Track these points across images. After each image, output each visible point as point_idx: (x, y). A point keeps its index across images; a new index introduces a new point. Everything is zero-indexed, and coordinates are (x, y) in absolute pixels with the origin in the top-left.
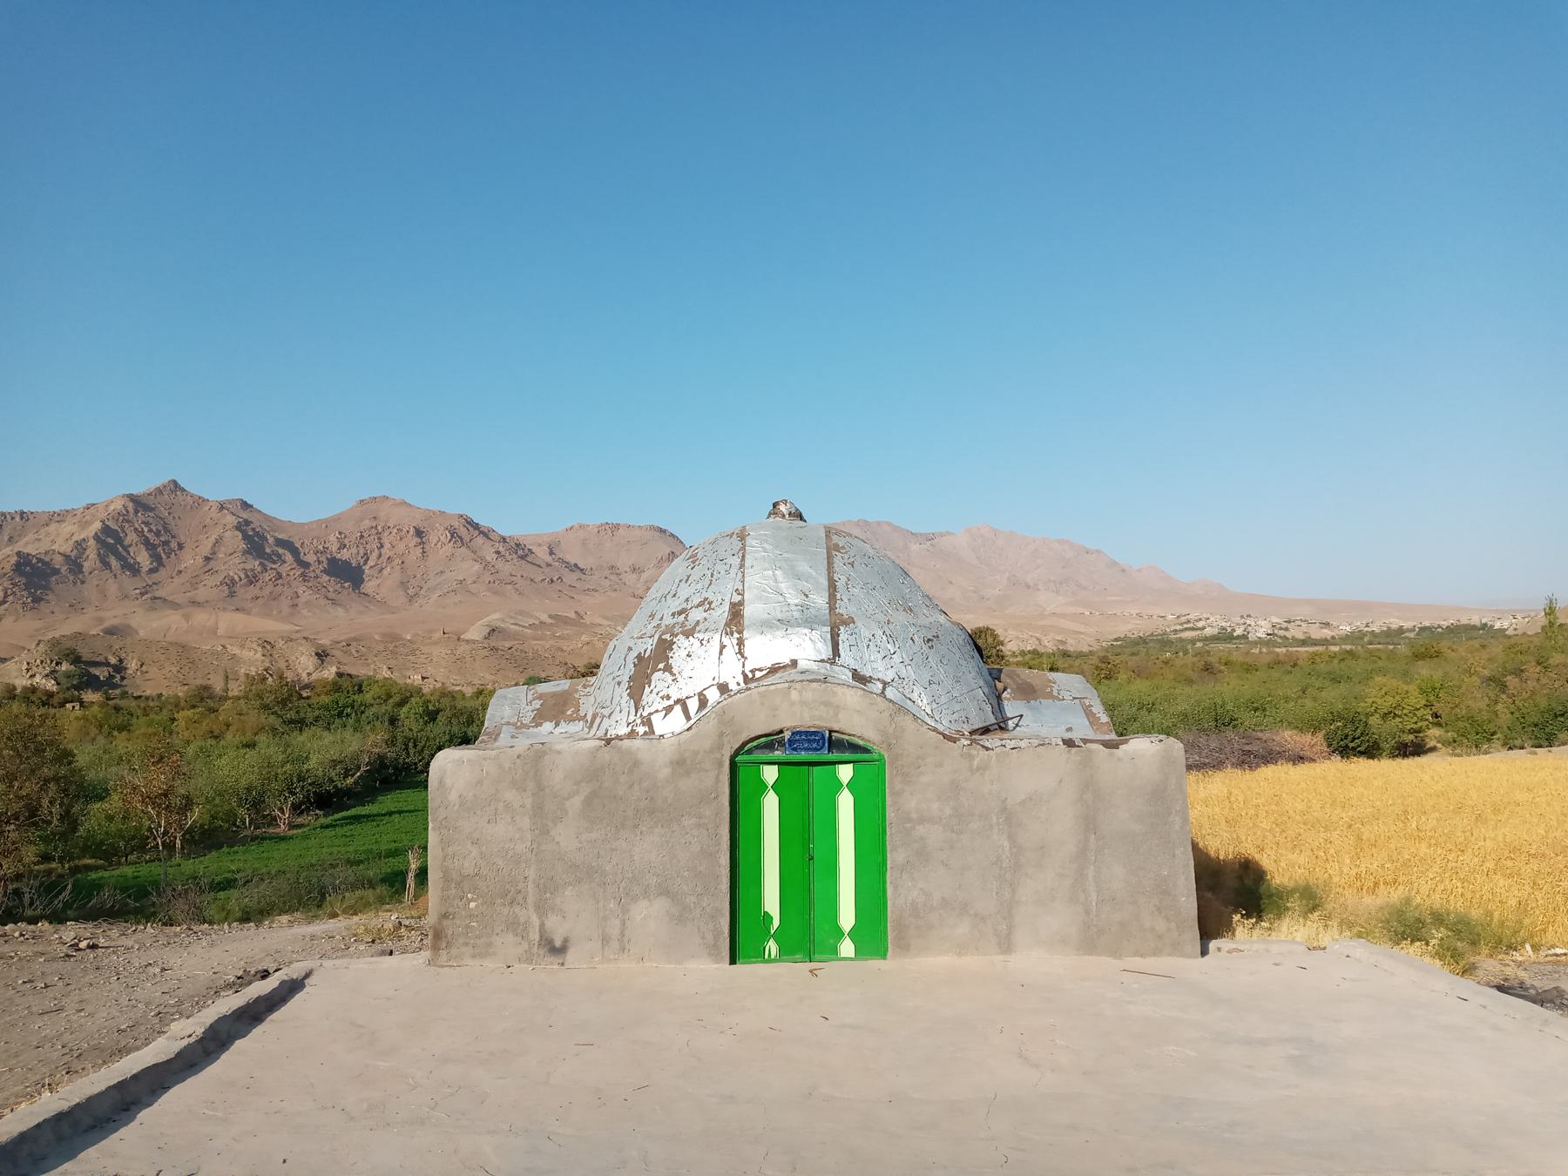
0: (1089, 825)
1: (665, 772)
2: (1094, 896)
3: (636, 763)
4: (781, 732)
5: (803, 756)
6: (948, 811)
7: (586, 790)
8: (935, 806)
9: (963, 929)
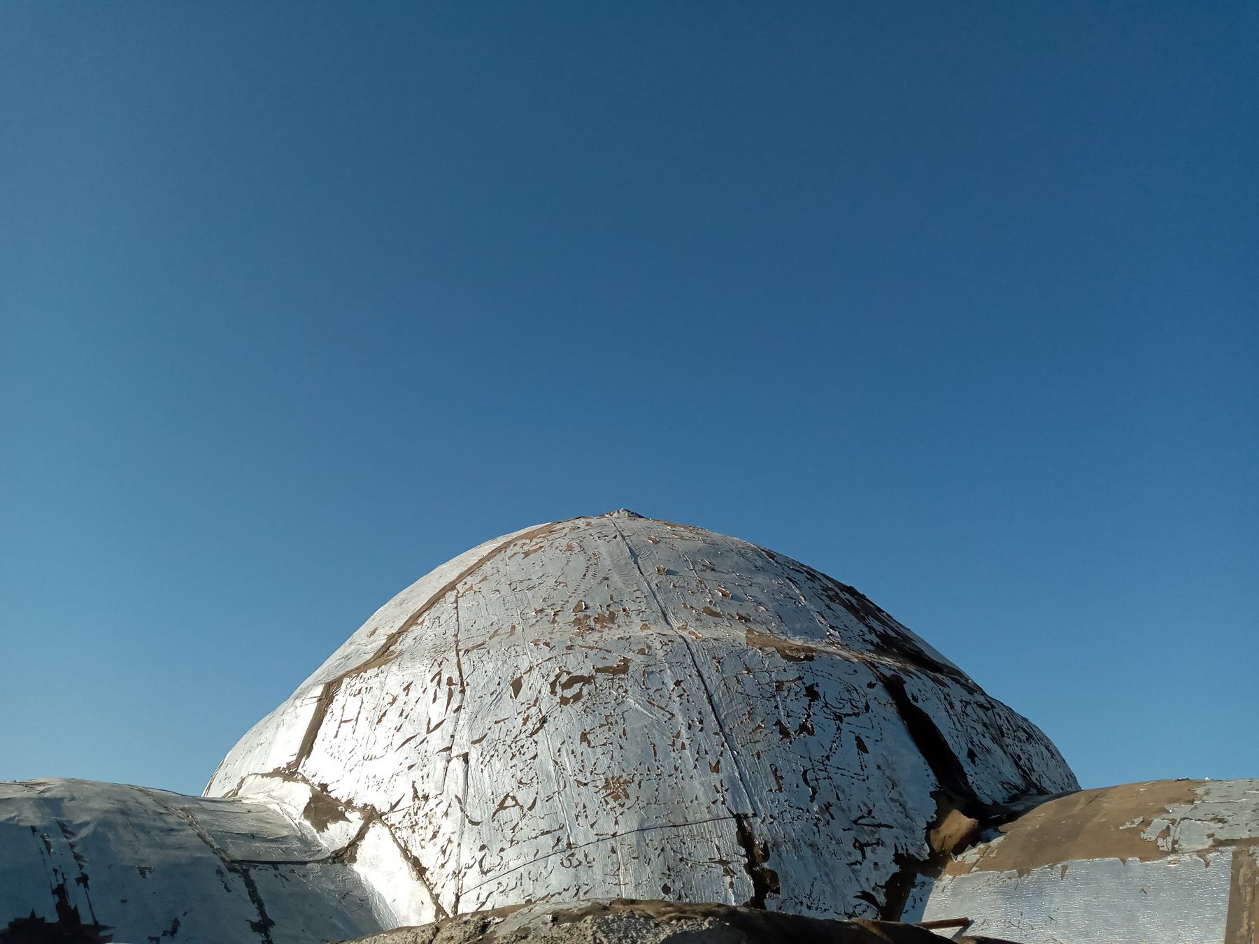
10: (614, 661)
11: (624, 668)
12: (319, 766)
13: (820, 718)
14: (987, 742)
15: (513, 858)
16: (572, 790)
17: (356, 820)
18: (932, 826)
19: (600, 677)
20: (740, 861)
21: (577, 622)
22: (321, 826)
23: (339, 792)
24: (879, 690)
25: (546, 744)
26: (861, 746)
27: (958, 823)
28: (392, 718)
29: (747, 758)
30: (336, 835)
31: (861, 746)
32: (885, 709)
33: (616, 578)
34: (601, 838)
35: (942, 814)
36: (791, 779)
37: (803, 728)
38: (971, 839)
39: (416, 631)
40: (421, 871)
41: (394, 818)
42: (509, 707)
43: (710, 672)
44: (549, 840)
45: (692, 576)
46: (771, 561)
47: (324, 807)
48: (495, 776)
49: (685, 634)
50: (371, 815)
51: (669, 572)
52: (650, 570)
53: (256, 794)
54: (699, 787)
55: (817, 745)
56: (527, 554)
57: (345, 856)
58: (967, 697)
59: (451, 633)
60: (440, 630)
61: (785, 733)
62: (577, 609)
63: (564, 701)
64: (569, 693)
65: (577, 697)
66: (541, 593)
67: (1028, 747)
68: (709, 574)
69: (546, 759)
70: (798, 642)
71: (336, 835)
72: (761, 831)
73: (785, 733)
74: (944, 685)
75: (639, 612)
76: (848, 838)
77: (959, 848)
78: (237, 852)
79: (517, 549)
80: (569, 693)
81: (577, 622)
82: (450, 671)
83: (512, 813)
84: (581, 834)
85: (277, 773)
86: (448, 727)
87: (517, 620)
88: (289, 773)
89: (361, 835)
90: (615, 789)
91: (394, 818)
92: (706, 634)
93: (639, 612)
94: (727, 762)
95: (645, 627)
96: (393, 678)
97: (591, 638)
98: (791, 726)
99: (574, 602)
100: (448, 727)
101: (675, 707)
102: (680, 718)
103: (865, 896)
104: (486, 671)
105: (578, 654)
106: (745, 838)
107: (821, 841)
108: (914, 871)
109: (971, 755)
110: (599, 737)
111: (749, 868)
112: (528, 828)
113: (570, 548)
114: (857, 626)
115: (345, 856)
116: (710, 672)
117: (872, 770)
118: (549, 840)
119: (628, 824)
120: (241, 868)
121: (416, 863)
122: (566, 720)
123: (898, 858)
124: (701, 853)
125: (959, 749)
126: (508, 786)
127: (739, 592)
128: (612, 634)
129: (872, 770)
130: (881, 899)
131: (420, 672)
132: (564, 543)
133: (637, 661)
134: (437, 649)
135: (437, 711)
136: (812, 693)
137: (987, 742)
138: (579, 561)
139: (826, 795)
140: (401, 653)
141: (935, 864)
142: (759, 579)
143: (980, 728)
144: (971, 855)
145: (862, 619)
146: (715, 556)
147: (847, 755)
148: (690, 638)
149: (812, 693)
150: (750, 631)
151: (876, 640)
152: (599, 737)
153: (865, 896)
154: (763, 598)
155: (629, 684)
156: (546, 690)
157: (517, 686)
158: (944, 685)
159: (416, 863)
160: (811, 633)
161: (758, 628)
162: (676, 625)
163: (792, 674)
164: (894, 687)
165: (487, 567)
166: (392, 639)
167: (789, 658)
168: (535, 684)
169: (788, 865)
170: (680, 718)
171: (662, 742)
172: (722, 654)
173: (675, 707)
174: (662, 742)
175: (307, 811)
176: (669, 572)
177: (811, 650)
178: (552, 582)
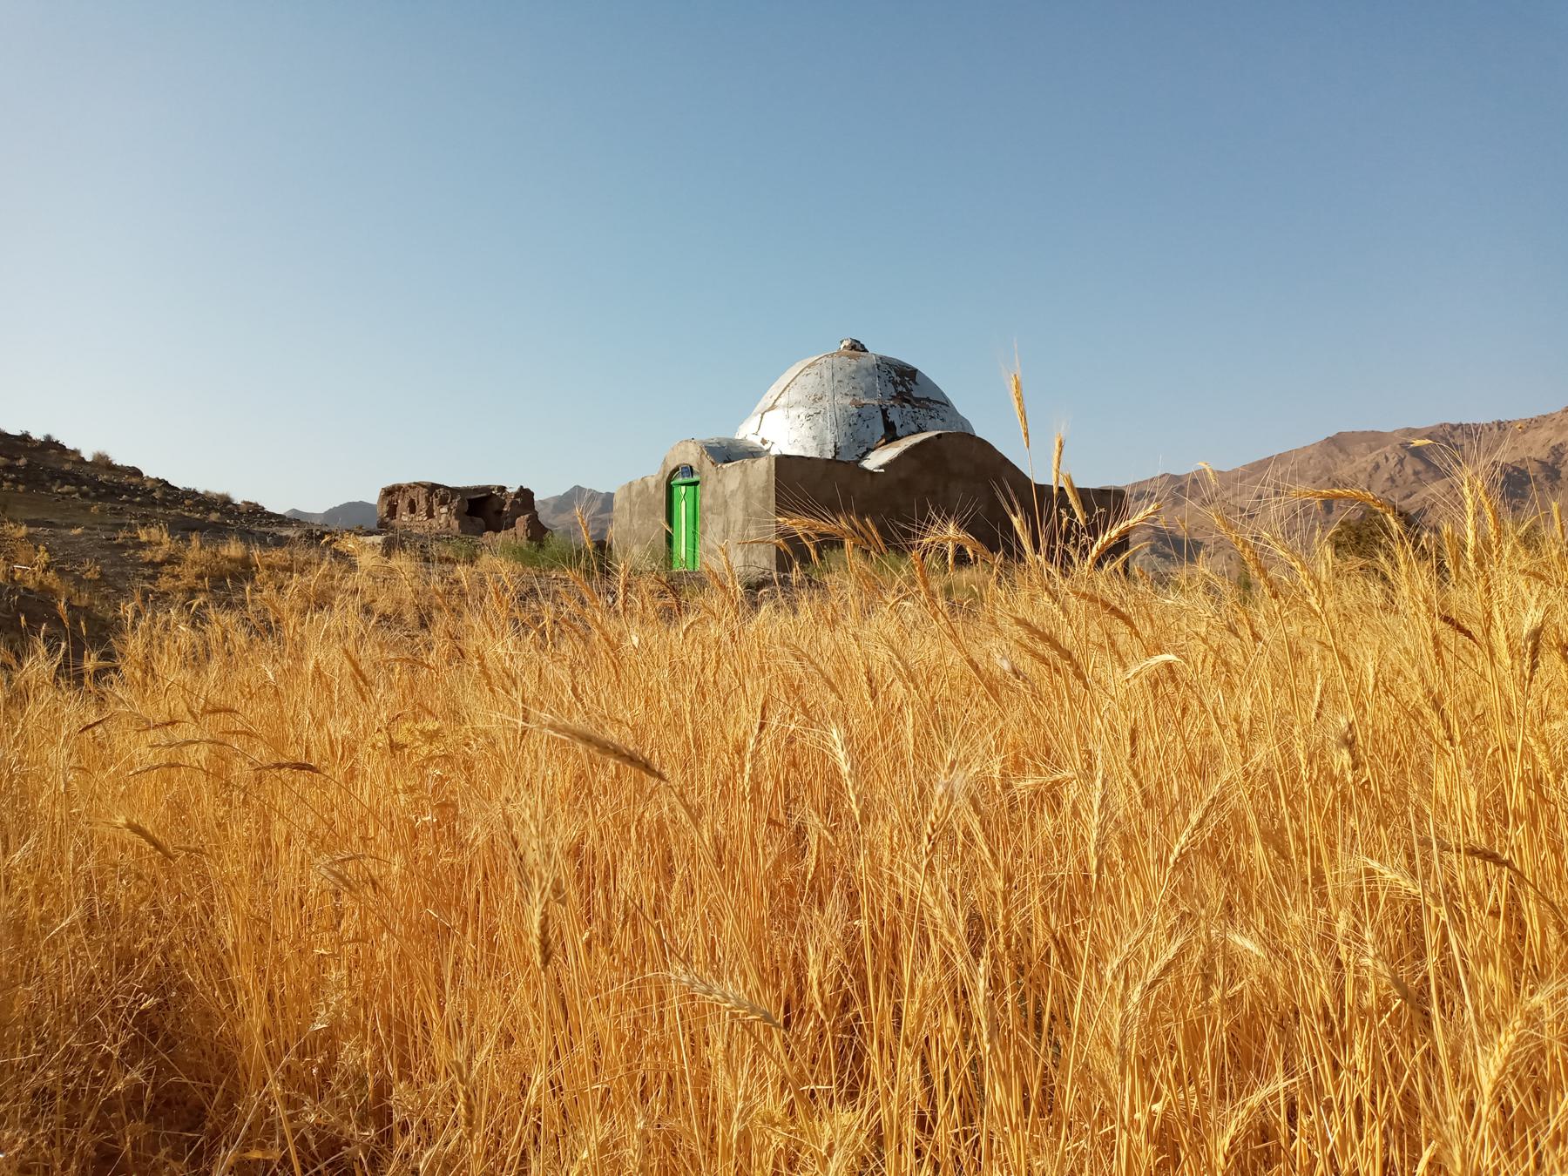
0: (746, 509)
4: (676, 469)
5: (687, 480)
32: (879, 416)
47: (764, 442)
54: (829, 437)
71: (766, 447)
104: (793, 413)
108: (869, 450)
114: (891, 390)
122: (808, 424)
125: (897, 425)
164: (884, 412)
169: (843, 451)
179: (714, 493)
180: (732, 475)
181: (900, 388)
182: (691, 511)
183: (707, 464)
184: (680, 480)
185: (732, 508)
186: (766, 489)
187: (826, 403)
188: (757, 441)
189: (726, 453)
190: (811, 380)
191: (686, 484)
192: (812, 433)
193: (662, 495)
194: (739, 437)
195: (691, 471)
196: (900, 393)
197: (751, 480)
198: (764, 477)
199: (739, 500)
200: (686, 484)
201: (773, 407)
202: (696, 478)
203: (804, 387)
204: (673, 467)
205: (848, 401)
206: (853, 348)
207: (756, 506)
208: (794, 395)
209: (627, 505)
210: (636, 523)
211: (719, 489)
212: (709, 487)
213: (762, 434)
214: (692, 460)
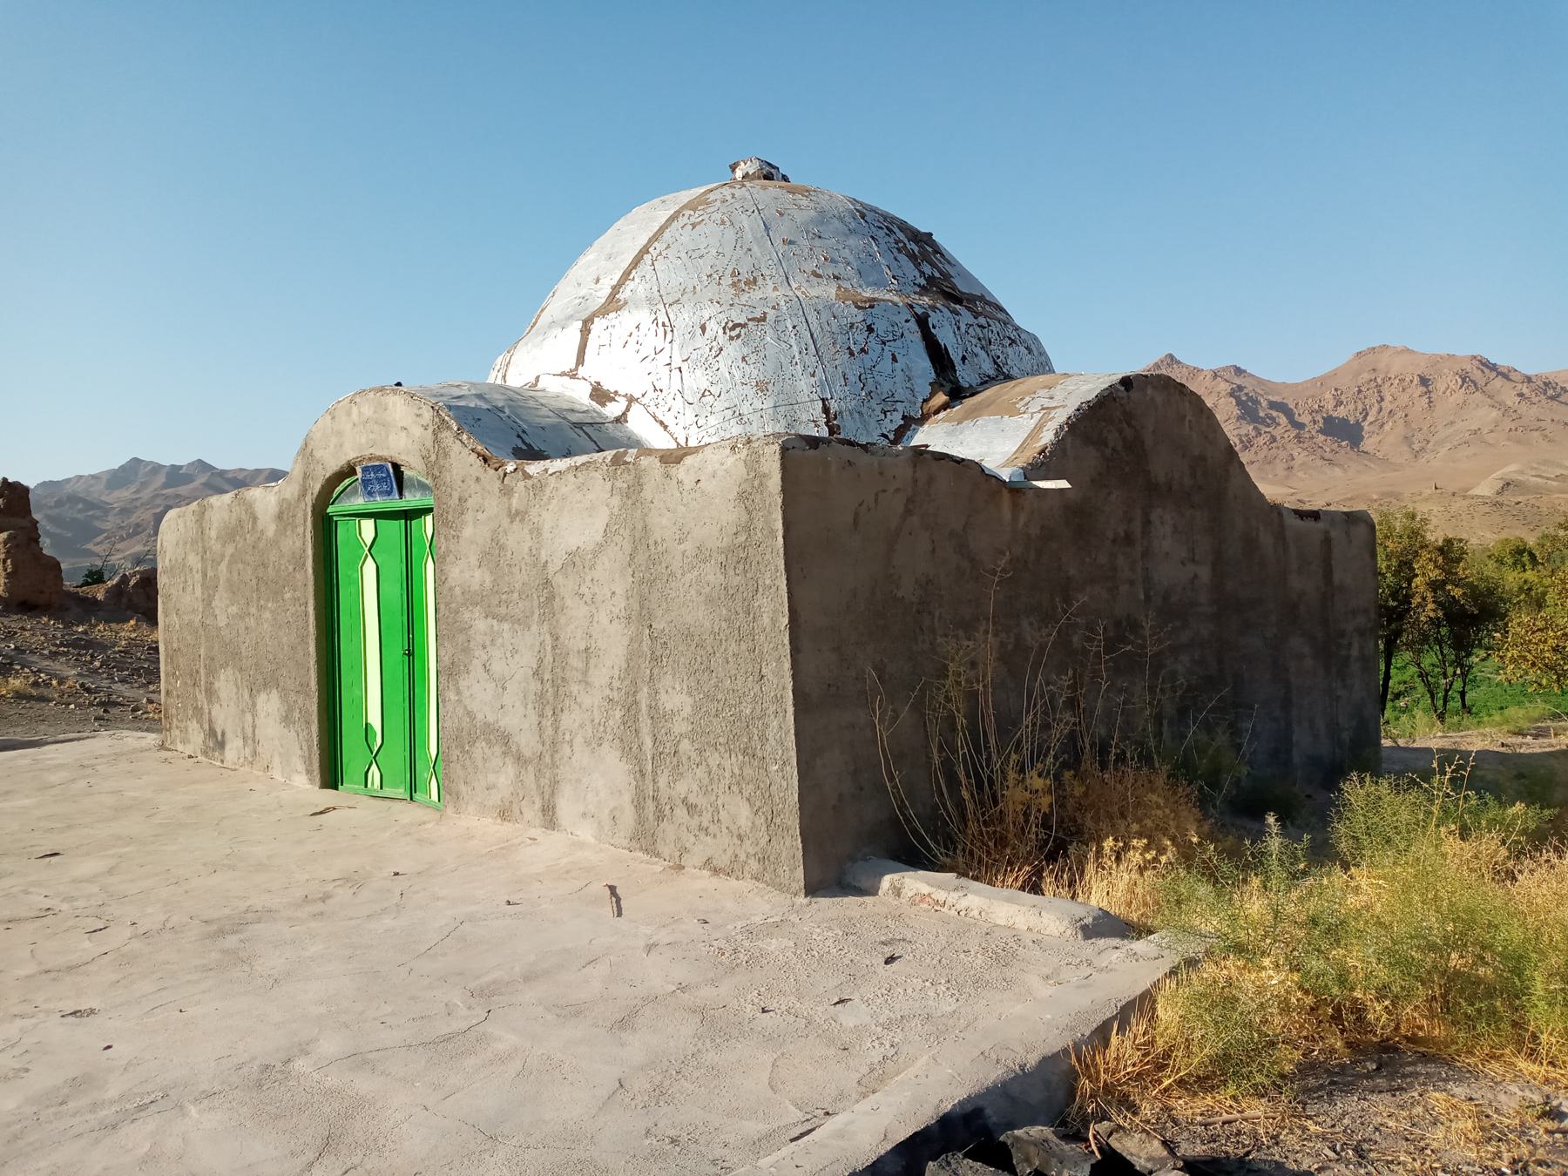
0: (641, 615)
1: (271, 530)
2: (648, 742)
3: (255, 519)
4: (349, 471)
5: (381, 503)
6: (488, 584)
7: (230, 550)
8: (477, 574)
9: (503, 777)
10: (758, 315)
11: (763, 319)
12: (594, 369)
13: (874, 345)
14: (978, 350)
15: (712, 420)
16: (739, 387)
17: (623, 403)
18: (925, 401)
19: (751, 324)
20: (822, 420)
21: (734, 285)
22: (603, 405)
23: (607, 385)
24: (913, 325)
25: (723, 363)
26: (894, 359)
27: (941, 398)
28: (632, 345)
29: (829, 369)
30: (613, 410)
31: (894, 359)
32: (916, 337)
33: (755, 249)
34: (755, 411)
35: (932, 394)
36: (853, 379)
37: (863, 350)
38: (945, 407)
39: (630, 285)
40: (666, 427)
41: (644, 401)
42: (700, 341)
43: (812, 318)
44: (730, 412)
45: (804, 243)
46: (864, 213)
47: (600, 395)
48: (697, 380)
49: (799, 293)
50: (631, 400)
51: (791, 242)
52: (778, 242)
53: (553, 386)
54: (804, 384)
55: (867, 360)
56: (694, 226)
57: (621, 419)
58: (971, 320)
59: (655, 289)
60: (648, 286)
61: (852, 354)
62: (733, 275)
63: (731, 338)
64: (733, 334)
65: (738, 336)
66: (709, 260)
67: (1010, 350)
68: (817, 242)
69: (724, 370)
70: (868, 293)
71: (613, 410)
72: (834, 406)
73: (852, 354)
74: (958, 314)
75: (772, 277)
76: (878, 409)
77: (937, 412)
78: (574, 418)
79: (685, 220)
80: (733, 334)
81: (734, 285)
82: (662, 318)
83: (710, 399)
84: (745, 409)
85: (563, 374)
86: (667, 352)
87: (696, 282)
88: (572, 375)
89: (628, 409)
90: (761, 387)
91: (644, 401)
92: (813, 292)
93: (772, 277)
94: (819, 372)
95: (775, 289)
96: (624, 321)
97: (744, 298)
98: (855, 349)
99: (730, 270)
100: (667, 352)
101: (793, 342)
102: (795, 348)
103: (884, 435)
104: (684, 318)
105: (737, 308)
106: (826, 410)
107: (864, 410)
108: (910, 423)
109: (964, 358)
110: (752, 358)
111: (827, 424)
112: (719, 406)
113: (723, 223)
115: (621, 419)
116: (812, 318)
117: (898, 372)
118: (730, 412)
119: (769, 403)
120: (578, 426)
121: (662, 423)
122: (733, 350)
123: (904, 417)
124: (804, 417)
125: (955, 356)
126: (705, 385)
127: (836, 256)
128: (756, 295)
129: (898, 372)
130: (892, 437)
131: (644, 316)
132: (717, 216)
133: (771, 314)
134: (649, 300)
135: (659, 342)
136: (870, 329)
137: (978, 350)
138: (730, 234)
139: (870, 386)
140: (626, 303)
141: (924, 419)
142: (852, 241)
143: (974, 341)
144: (942, 415)
145: (917, 266)
146: (822, 223)
147: (886, 364)
148: (802, 297)
149: (870, 329)
150: (839, 287)
151: (923, 282)
152: (752, 358)
153: (884, 435)
154: (851, 258)
155: (767, 328)
156: (721, 331)
157: (703, 328)
158: (958, 314)
159: (662, 423)
160: (877, 284)
161: (846, 285)
162: (794, 285)
163: (860, 318)
164: (922, 321)
165: (667, 234)
166: (616, 289)
167: (859, 308)
168: (714, 328)
170: (795, 348)
171: (785, 361)
172: (820, 307)
173: (793, 342)
174: (785, 361)
175: (591, 396)
176: (791, 242)
177: (874, 300)
178: (714, 252)
179: (494, 554)
180: (571, 507)
181: (927, 269)
182: (395, 591)
183: (462, 459)
184: (359, 502)
185: (576, 611)
186: (738, 556)
187: (769, 292)
188: (579, 394)
189: (520, 435)
190: (710, 236)
191: (376, 516)
192: (753, 372)
193: (302, 539)
194: (516, 380)
195: (397, 477)
196: (931, 280)
197: (662, 524)
198: (729, 514)
199: (611, 582)
200: (376, 516)
201: (613, 303)
202: (412, 500)
203: (694, 255)
204: (334, 465)
205: (831, 290)
206: (768, 177)
207: (690, 605)
208: (669, 272)
209: (193, 560)
210: (224, 610)
211: (517, 540)
212: (473, 532)
213: (594, 369)
214: (403, 435)
